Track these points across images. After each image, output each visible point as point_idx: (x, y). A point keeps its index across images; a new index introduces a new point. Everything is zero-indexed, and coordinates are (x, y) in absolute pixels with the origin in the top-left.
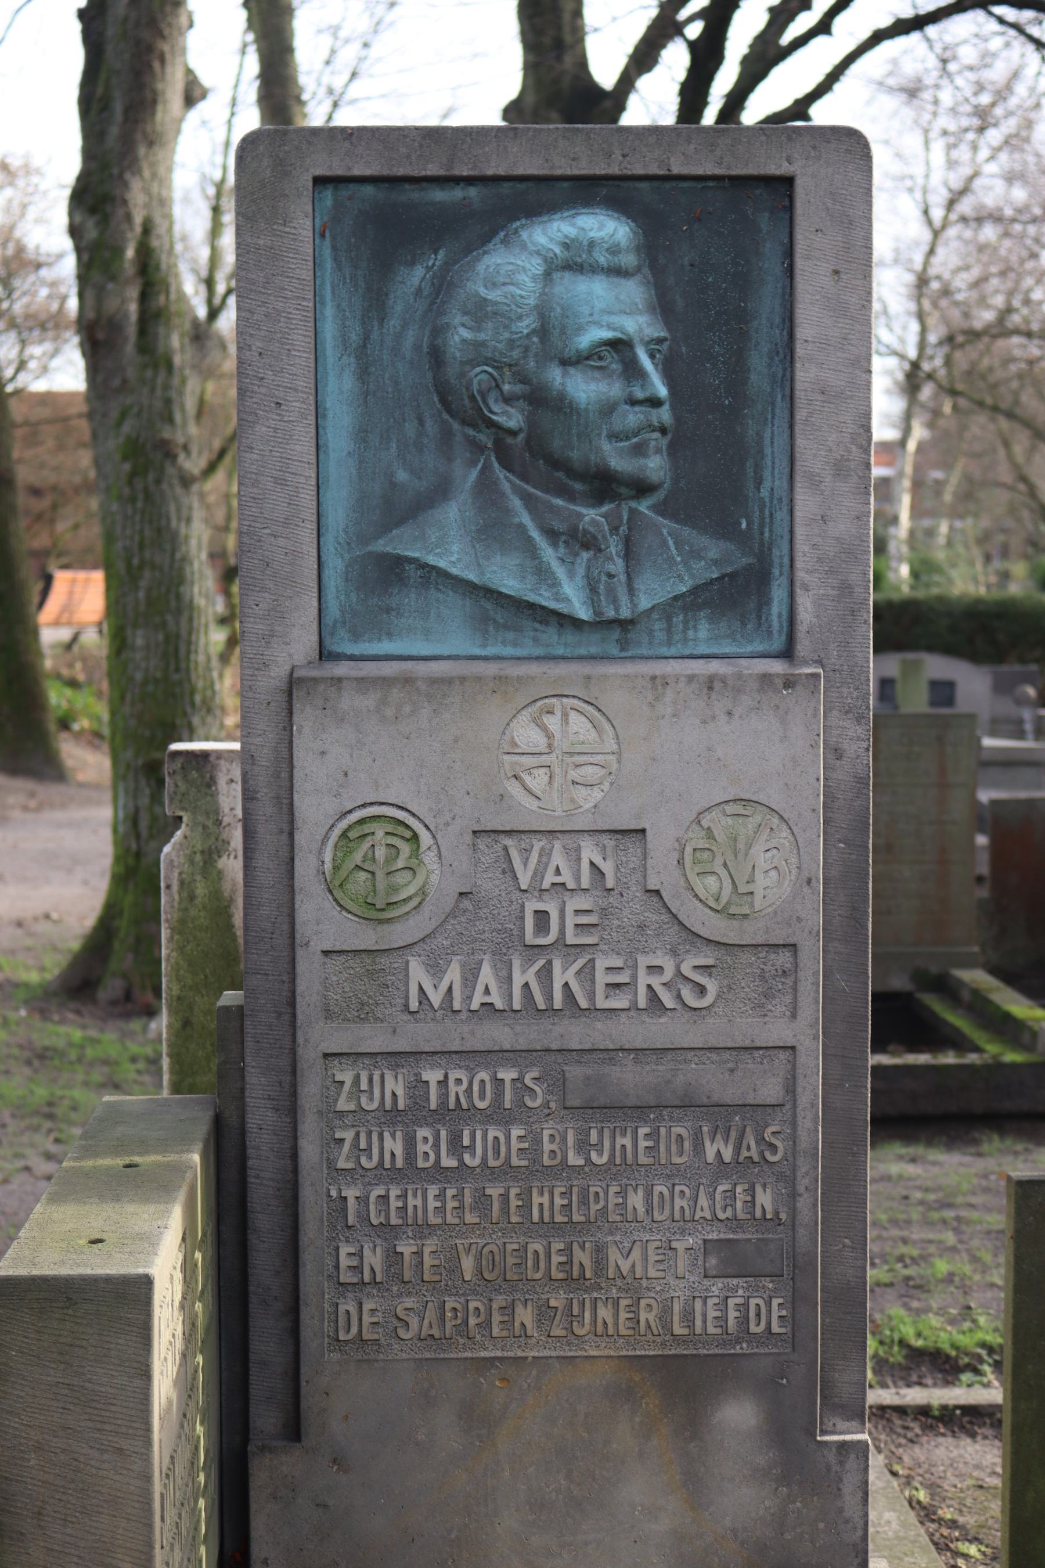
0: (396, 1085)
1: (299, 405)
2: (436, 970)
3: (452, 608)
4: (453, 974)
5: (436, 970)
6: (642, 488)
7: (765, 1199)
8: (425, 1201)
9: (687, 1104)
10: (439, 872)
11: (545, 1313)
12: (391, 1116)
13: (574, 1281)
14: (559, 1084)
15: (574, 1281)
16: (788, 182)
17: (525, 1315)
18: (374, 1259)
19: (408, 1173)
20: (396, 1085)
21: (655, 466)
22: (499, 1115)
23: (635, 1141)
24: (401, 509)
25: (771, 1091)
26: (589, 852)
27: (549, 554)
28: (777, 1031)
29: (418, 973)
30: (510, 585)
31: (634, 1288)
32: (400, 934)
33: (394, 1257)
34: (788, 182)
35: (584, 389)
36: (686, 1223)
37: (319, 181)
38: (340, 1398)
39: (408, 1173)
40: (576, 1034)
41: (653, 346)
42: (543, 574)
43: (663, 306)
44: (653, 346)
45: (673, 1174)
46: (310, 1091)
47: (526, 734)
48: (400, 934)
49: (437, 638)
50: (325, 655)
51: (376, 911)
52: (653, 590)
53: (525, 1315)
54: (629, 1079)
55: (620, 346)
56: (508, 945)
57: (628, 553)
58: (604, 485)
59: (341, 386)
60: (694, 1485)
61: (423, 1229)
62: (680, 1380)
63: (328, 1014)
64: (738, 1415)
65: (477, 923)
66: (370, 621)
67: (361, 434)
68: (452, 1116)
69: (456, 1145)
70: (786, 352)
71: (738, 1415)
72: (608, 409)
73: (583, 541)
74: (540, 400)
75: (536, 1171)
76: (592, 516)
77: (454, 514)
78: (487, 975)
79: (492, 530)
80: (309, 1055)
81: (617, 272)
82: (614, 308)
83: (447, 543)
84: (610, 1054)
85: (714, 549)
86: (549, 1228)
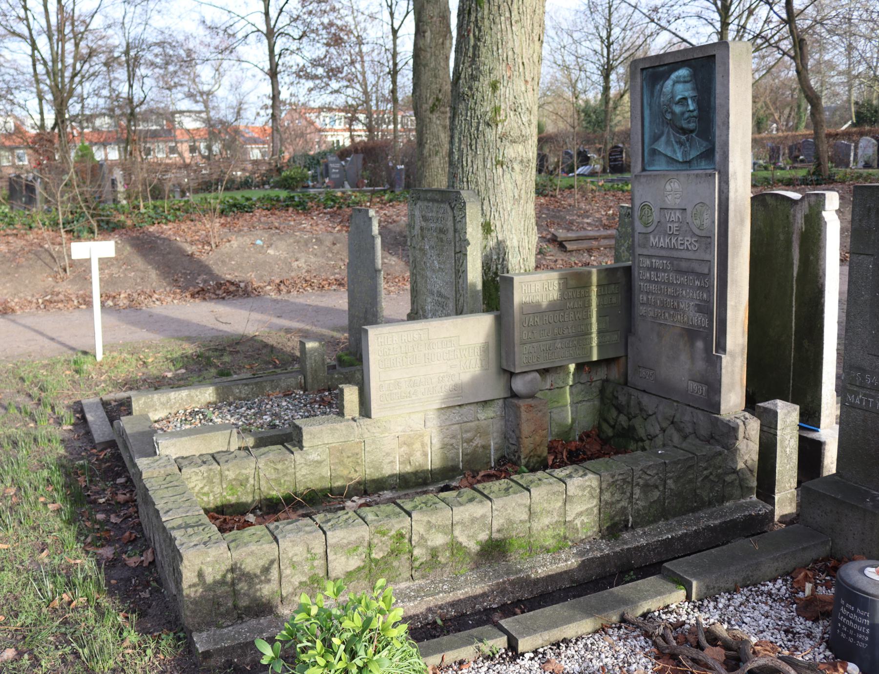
2: (655, 238)
3: (663, 159)
4: (657, 239)
5: (655, 238)
6: (692, 131)
7: (705, 296)
8: (653, 287)
9: (693, 272)
10: (655, 216)
11: (670, 315)
13: (674, 309)
16: (714, 56)
17: (667, 315)
19: (650, 281)
21: (692, 126)
22: (664, 271)
23: (683, 279)
24: (656, 138)
25: (706, 271)
26: (678, 214)
27: (676, 147)
28: (707, 257)
30: (669, 154)
32: (650, 229)
33: (648, 299)
34: (714, 56)
35: (678, 109)
36: (692, 299)
37: (642, 70)
38: (641, 328)
39: (650, 281)
40: (675, 254)
41: (693, 98)
42: (674, 151)
43: (696, 88)
44: (693, 98)
45: (691, 288)
48: (650, 229)
49: (660, 166)
50: (644, 170)
51: (646, 225)
52: (694, 154)
53: (667, 315)
54: (684, 265)
55: (685, 99)
56: (665, 234)
58: (684, 131)
59: (647, 113)
60: (692, 358)
61: (653, 294)
62: (691, 334)
63: (639, 246)
64: (700, 344)
65: (661, 228)
66: (651, 163)
67: (650, 122)
68: (656, 269)
69: (657, 277)
72: (683, 113)
73: (681, 144)
74: (673, 113)
75: (669, 284)
76: (684, 137)
77: (663, 139)
78: (662, 240)
79: (668, 143)
80: (637, 254)
81: (685, 82)
82: (683, 90)
83: (661, 146)
84: (680, 259)
85: (705, 144)
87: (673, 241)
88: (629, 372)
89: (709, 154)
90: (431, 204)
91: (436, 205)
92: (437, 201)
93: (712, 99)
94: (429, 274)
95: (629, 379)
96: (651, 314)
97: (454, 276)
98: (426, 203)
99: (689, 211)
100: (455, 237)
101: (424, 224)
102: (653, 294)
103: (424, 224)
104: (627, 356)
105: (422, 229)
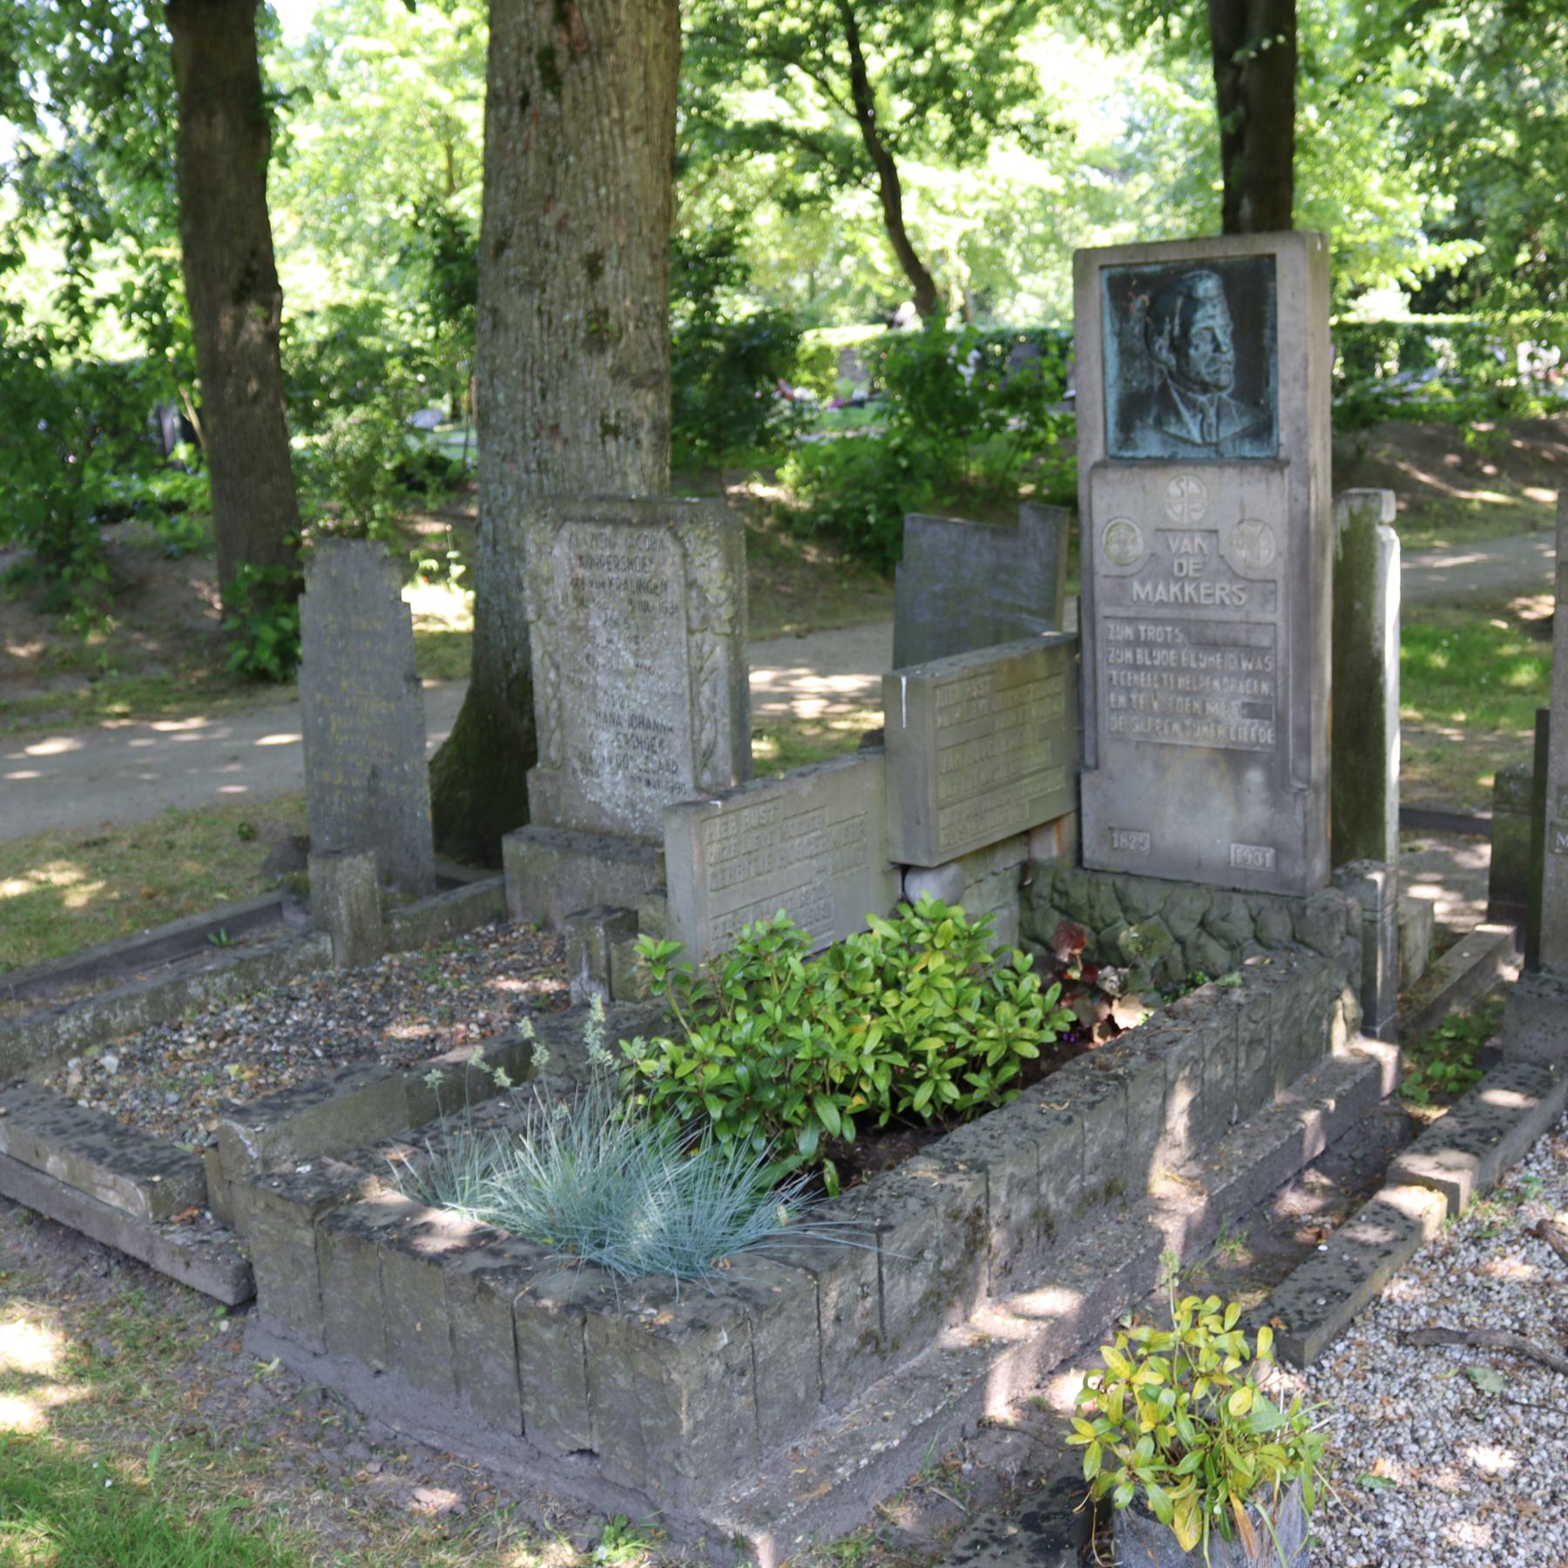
0: (1128, 631)
1: (1095, 358)
2: (1143, 584)
4: (1149, 587)
5: (1143, 584)
7: (1265, 687)
8: (1141, 678)
11: (1184, 727)
12: (1128, 644)
13: (1194, 715)
14: (1188, 634)
15: (1194, 715)
17: (1176, 727)
18: (1122, 700)
19: (1135, 667)
20: (1128, 631)
22: (1166, 645)
23: (1215, 659)
25: (1265, 641)
26: (1198, 540)
28: (1269, 618)
29: (1136, 587)
31: (1217, 721)
33: (1129, 700)
34: (1272, 257)
36: (1234, 695)
38: (1113, 755)
40: (1193, 614)
45: (1231, 674)
46: (1099, 629)
47: (1174, 489)
48: (1130, 570)
54: (1212, 633)
56: (1169, 577)
57: (1218, 416)
59: (1112, 347)
60: (1239, 803)
61: (1140, 690)
64: (1255, 776)
65: (1158, 567)
68: (1150, 645)
69: (1151, 657)
70: (1274, 328)
71: (1255, 776)
75: (1180, 670)
78: (1161, 588)
80: (1099, 617)
84: (1207, 622)
86: (1185, 693)
87: (1189, 589)
88: (1086, 841)
89: (1263, 428)
90: (608, 530)
91: (625, 531)
92: (629, 523)
93: (1267, 332)
94: (602, 680)
95: (1087, 854)
96: (1138, 728)
97: (685, 681)
98: (591, 528)
99: (1223, 535)
100: (687, 599)
101: (581, 572)
102: (1140, 690)
103: (581, 572)
104: (1078, 811)
105: (577, 583)
